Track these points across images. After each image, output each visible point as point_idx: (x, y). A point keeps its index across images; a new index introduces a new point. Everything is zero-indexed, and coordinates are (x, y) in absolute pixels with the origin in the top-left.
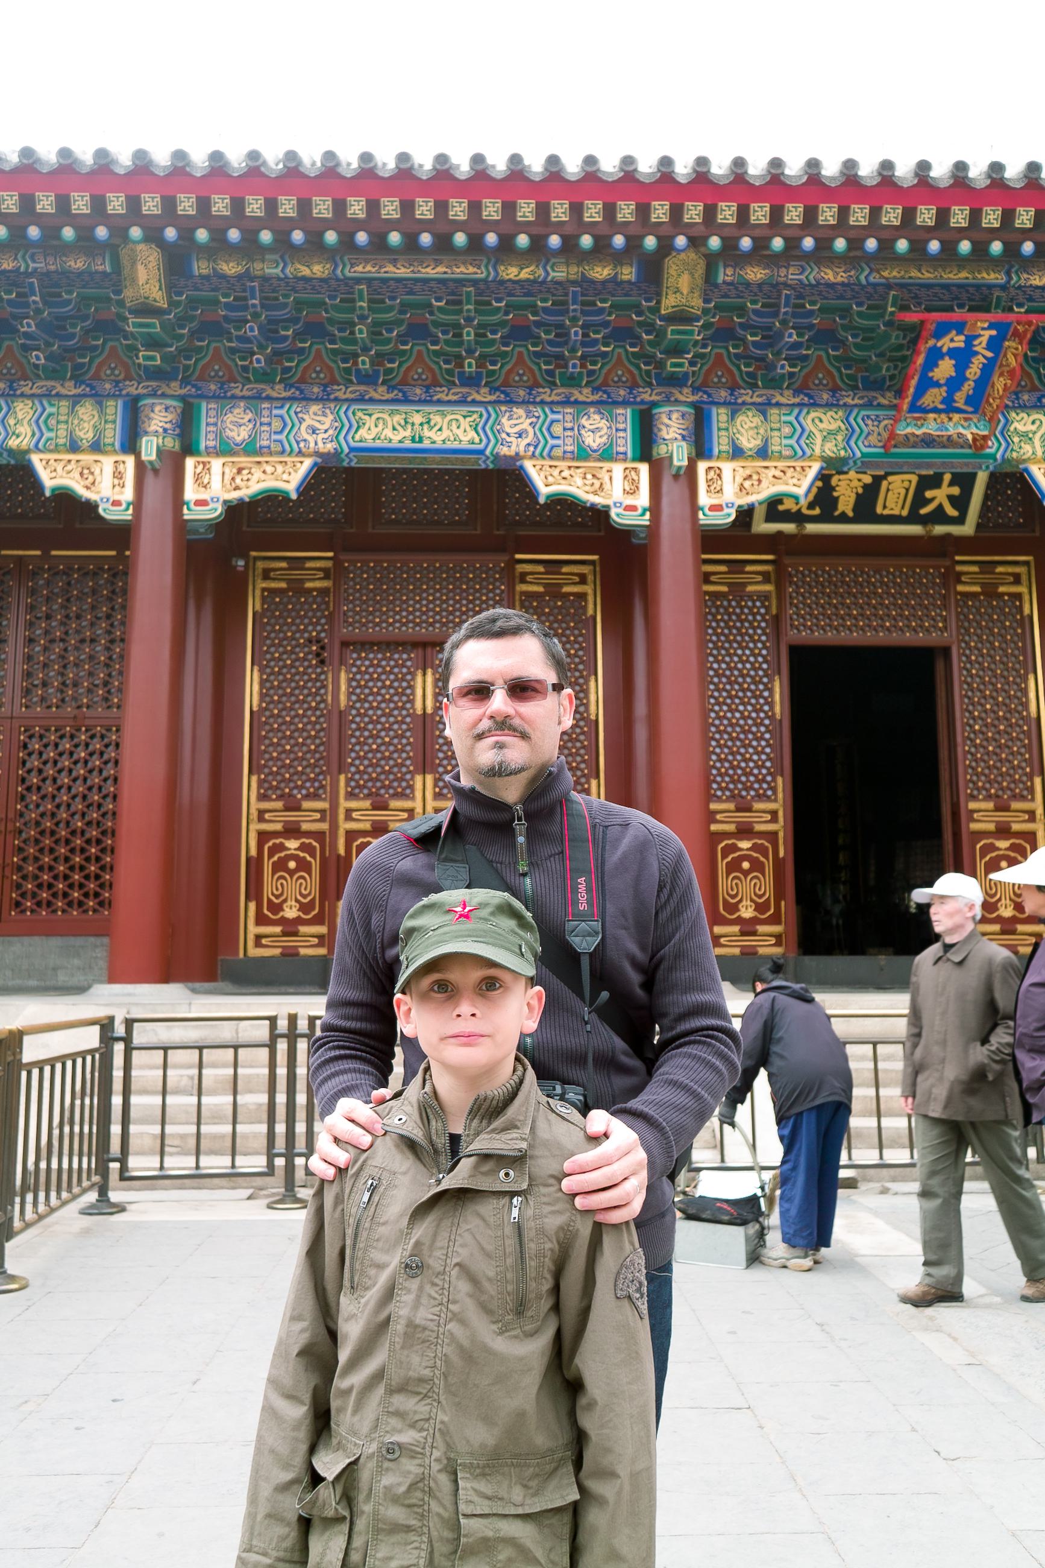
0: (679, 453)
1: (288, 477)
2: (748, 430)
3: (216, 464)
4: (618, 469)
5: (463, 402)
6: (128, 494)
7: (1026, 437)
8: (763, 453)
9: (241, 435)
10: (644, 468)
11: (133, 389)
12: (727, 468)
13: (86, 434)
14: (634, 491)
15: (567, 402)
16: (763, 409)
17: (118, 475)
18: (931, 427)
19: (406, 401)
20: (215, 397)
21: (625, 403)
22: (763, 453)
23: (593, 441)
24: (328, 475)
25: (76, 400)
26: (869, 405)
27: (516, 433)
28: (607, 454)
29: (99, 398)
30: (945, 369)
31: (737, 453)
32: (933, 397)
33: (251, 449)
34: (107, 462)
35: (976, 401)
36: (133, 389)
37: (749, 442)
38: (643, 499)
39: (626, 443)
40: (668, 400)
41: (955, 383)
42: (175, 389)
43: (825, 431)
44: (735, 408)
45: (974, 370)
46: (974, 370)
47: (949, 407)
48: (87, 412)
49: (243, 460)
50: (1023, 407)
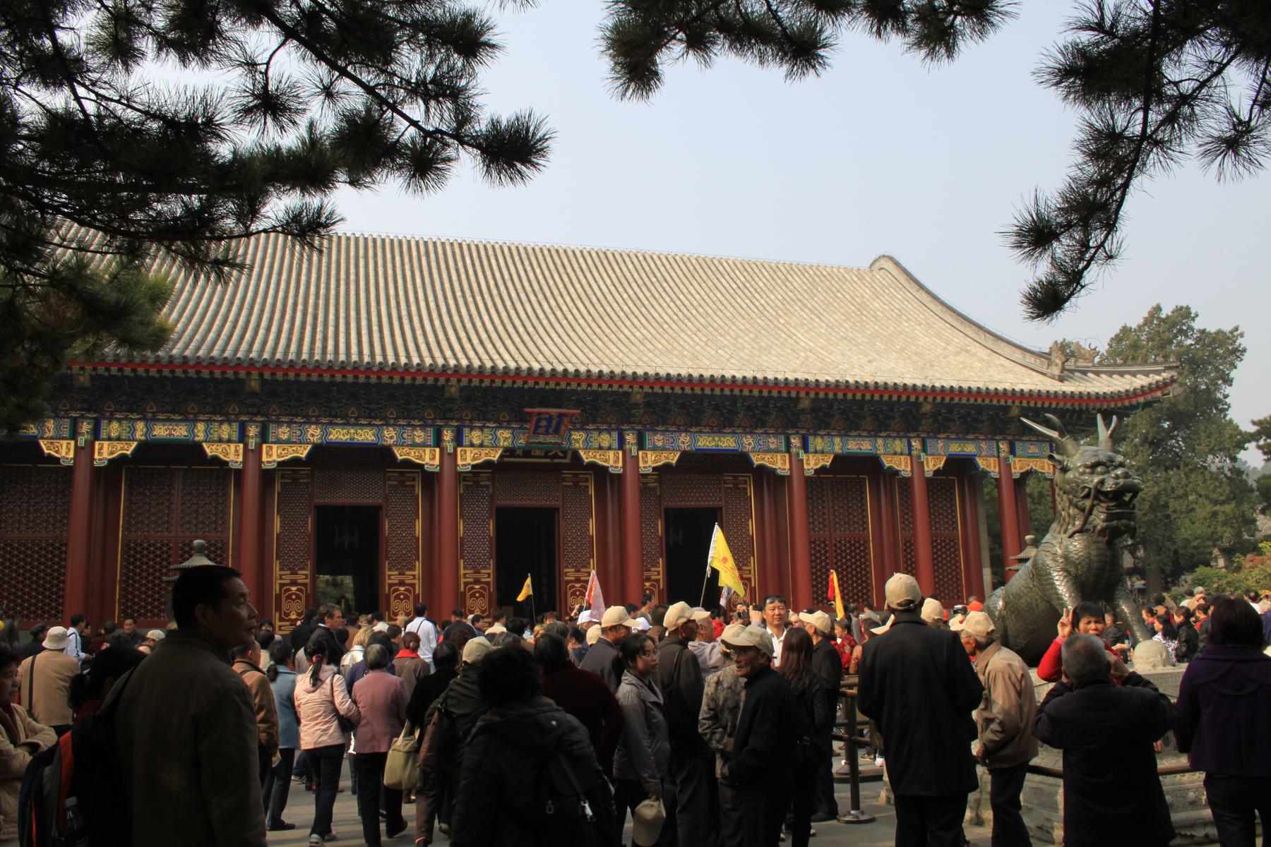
0: (450, 447)
1: (303, 452)
2: (476, 436)
3: (275, 447)
4: (428, 450)
5: (369, 425)
6: (241, 459)
7: (577, 441)
8: (481, 445)
9: (285, 437)
10: (438, 450)
11: (243, 418)
12: (468, 449)
13: (225, 437)
14: (433, 458)
15: (409, 425)
16: (481, 429)
17: (237, 451)
18: (541, 439)
19: (347, 424)
20: (274, 422)
21: (430, 426)
22: (481, 445)
23: (418, 440)
24: (317, 450)
25: (221, 423)
26: (521, 428)
27: (389, 435)
28: (424, 445)
29: (230, 422)
30: (544, 423)
31: (472, 445)
32: (540, 430)
33: (288, 442)
34: (233, 446)
35: (557, 431)
36: (243, 418)
37: (476, 442)
38: (437, 462)
39: (431, 441)
40: (447, 425)
41: (548, 427)
42: (259, 418)
43: (505, 437)
44: (472, 428)
45: (554, 423)
46: (554, 423)
47: (547, 433)
48: (225, 427)
49: (286, 446)
50: (577, 430)
